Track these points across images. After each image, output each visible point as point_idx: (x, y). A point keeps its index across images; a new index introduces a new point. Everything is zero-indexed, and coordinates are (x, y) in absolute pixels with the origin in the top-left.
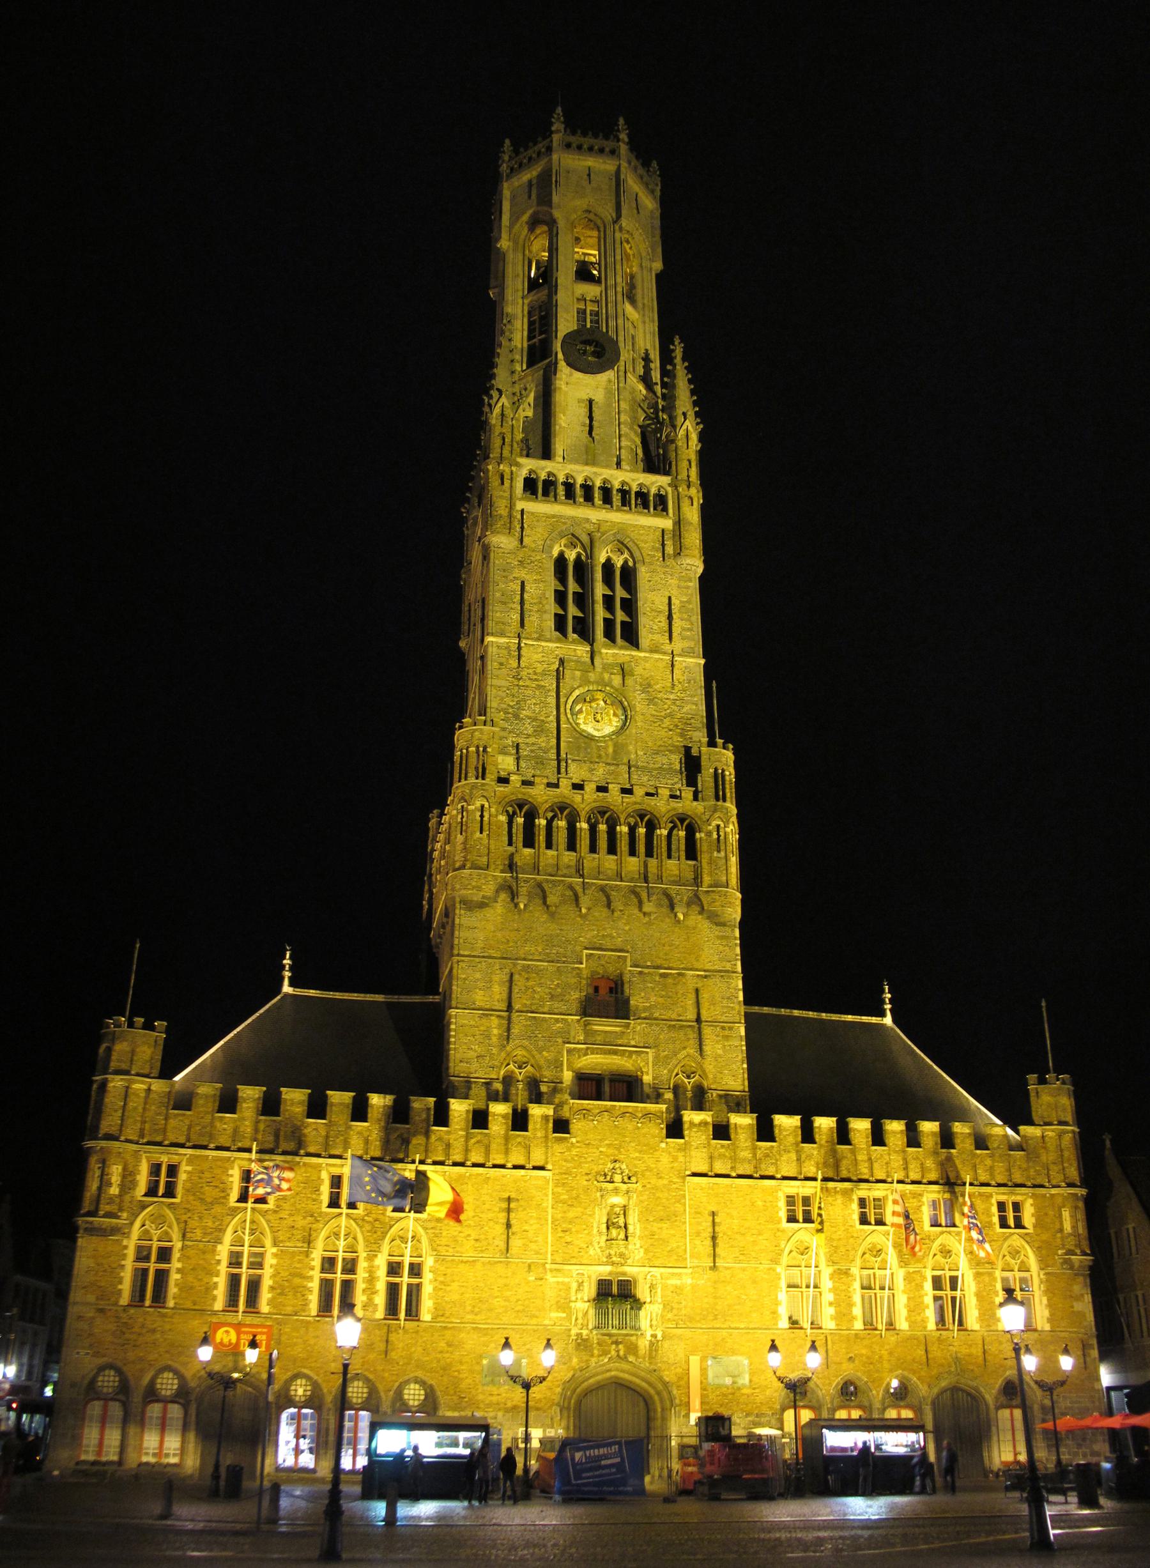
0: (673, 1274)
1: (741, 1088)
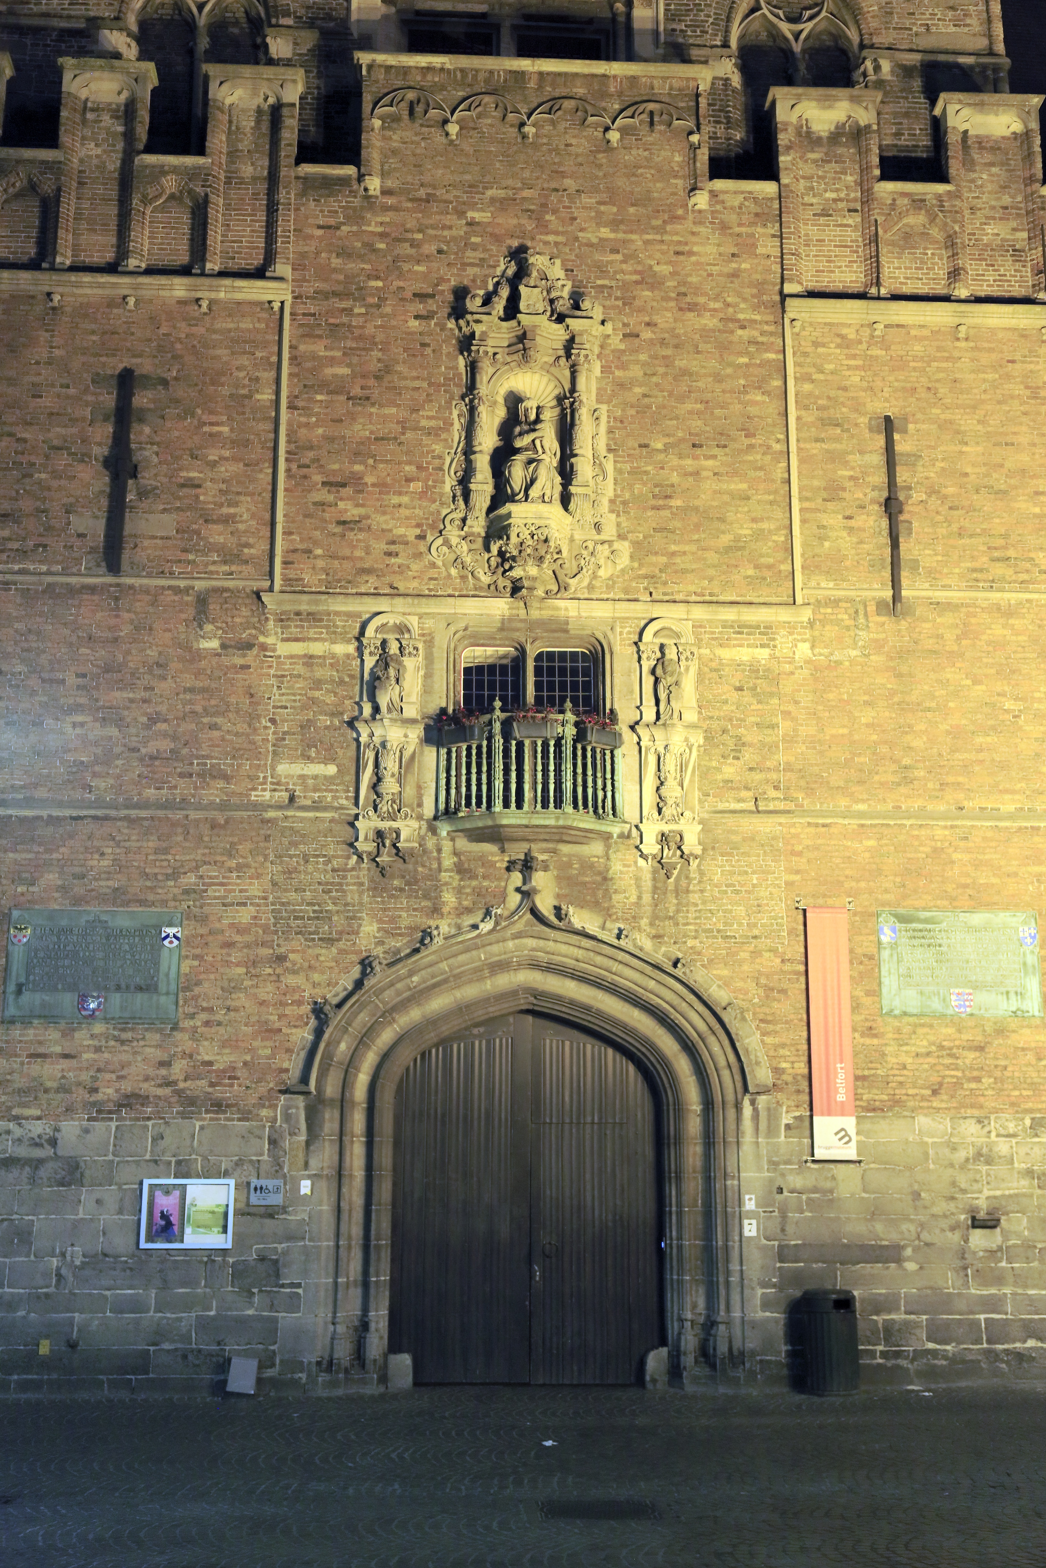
0: (741, 628)
1: (982, 43)
